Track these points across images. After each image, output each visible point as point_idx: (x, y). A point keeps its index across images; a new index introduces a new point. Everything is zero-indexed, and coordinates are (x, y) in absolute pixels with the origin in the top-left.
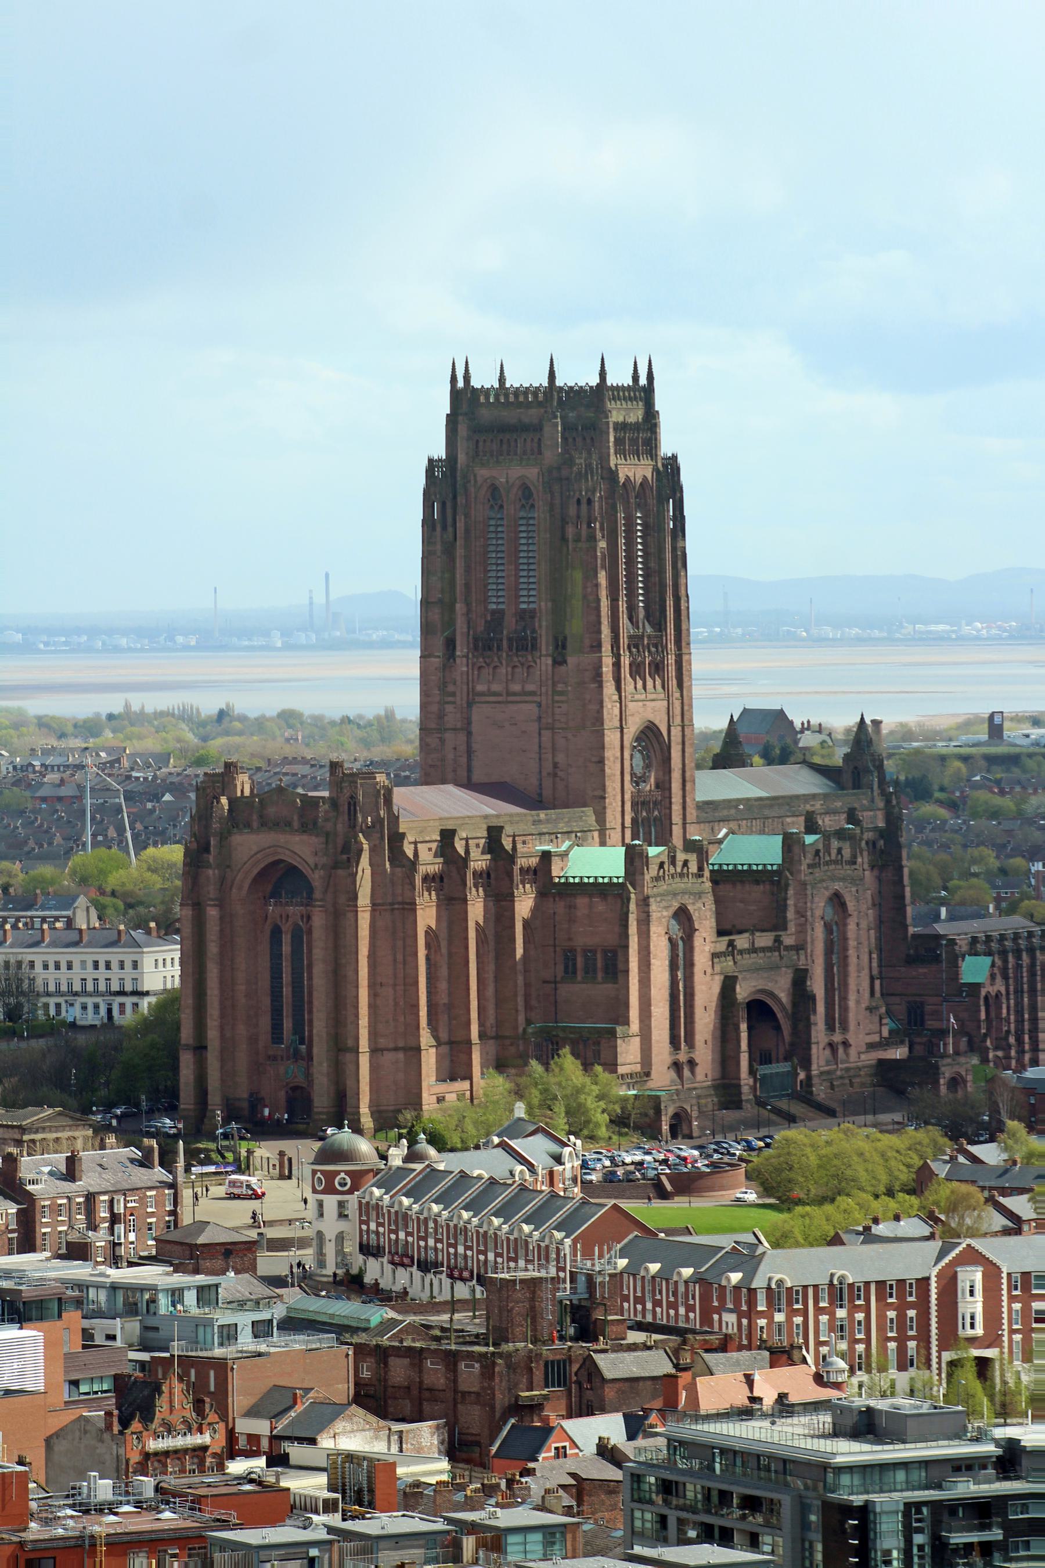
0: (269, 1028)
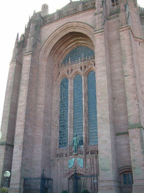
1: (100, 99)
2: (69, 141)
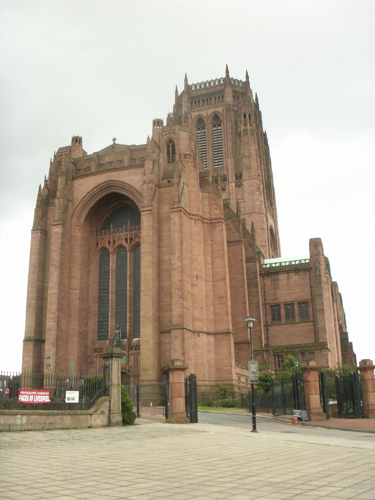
0: (96, 328)
1: (144, 295)
2: (109, 334)
